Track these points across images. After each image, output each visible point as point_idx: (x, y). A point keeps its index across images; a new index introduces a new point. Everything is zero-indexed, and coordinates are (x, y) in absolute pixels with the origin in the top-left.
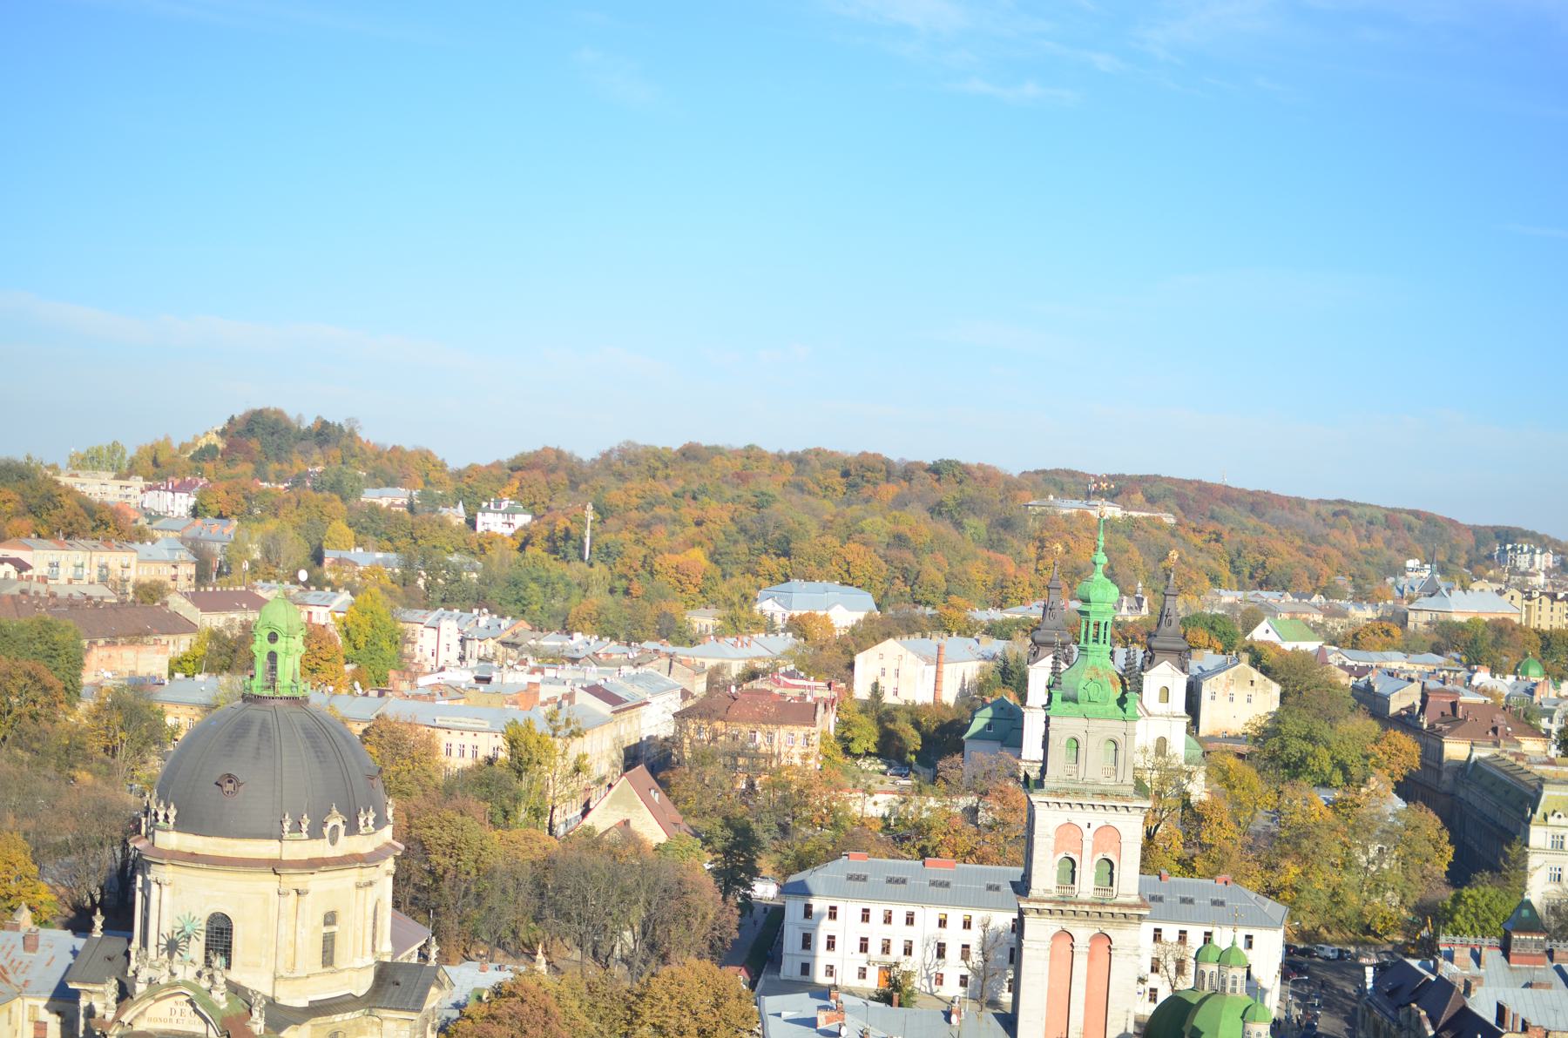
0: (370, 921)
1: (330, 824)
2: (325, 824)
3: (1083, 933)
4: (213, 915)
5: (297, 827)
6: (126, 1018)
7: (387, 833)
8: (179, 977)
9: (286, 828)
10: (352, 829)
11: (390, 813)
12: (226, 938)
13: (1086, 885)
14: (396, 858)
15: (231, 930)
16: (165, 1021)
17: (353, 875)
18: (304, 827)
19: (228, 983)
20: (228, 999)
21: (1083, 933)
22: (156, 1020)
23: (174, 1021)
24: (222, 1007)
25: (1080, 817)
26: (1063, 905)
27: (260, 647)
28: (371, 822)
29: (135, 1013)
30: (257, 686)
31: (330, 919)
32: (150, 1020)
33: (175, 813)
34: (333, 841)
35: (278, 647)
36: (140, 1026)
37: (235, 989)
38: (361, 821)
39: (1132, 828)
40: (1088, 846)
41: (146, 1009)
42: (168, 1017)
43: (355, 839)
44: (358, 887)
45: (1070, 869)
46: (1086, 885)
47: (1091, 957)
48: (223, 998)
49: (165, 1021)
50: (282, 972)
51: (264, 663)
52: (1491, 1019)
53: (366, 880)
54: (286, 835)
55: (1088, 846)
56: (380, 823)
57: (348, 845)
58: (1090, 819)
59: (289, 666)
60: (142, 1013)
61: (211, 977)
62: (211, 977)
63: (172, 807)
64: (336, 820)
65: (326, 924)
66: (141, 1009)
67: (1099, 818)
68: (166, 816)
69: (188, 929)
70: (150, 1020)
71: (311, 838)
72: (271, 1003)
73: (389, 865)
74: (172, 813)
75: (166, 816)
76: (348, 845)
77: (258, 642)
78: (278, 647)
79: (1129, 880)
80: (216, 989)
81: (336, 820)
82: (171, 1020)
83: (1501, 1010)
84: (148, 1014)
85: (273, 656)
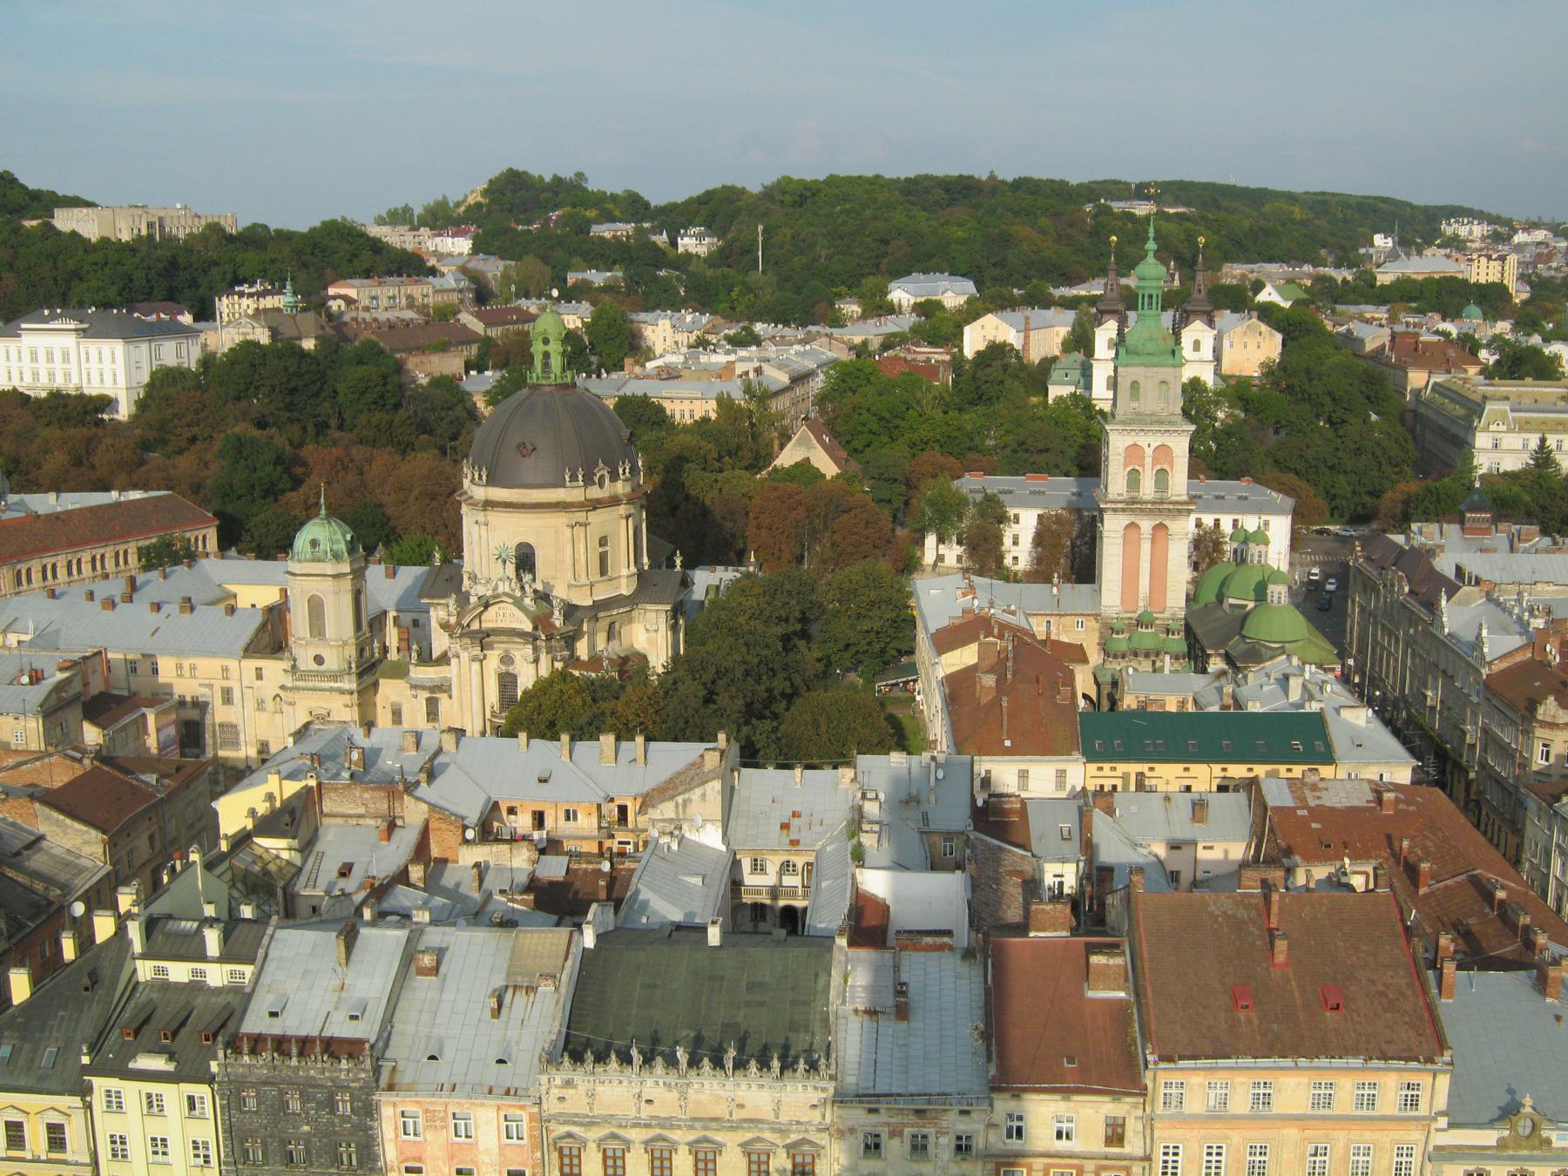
3: (1146, 525)
5: (574, 478)
9: (567, 479)
13: (1147, 490)
18: (580, 477)
21: (1146, 525)
25: (1142, 440)
26: (1133, 505)
31: (603, 541)
34: (601, 486)
38: (621, 471)
39: (1180, 446)
40: (1148, 460)
45: (1134, 479)
46: (1147, 490)
47: (1153, 541)
52: (1450, 573)
54: (568, 484)
55: (1148, 460)
58: (1149, 442)
59: (556, 362)
61: (522, 588)
62: (522, 588)
65: (601, 545)
67: (1156, 440)
68: (480, 477)
75: (480, 477)
79: (1179, 482)
81: (602, 471)
83: (1459, 571)
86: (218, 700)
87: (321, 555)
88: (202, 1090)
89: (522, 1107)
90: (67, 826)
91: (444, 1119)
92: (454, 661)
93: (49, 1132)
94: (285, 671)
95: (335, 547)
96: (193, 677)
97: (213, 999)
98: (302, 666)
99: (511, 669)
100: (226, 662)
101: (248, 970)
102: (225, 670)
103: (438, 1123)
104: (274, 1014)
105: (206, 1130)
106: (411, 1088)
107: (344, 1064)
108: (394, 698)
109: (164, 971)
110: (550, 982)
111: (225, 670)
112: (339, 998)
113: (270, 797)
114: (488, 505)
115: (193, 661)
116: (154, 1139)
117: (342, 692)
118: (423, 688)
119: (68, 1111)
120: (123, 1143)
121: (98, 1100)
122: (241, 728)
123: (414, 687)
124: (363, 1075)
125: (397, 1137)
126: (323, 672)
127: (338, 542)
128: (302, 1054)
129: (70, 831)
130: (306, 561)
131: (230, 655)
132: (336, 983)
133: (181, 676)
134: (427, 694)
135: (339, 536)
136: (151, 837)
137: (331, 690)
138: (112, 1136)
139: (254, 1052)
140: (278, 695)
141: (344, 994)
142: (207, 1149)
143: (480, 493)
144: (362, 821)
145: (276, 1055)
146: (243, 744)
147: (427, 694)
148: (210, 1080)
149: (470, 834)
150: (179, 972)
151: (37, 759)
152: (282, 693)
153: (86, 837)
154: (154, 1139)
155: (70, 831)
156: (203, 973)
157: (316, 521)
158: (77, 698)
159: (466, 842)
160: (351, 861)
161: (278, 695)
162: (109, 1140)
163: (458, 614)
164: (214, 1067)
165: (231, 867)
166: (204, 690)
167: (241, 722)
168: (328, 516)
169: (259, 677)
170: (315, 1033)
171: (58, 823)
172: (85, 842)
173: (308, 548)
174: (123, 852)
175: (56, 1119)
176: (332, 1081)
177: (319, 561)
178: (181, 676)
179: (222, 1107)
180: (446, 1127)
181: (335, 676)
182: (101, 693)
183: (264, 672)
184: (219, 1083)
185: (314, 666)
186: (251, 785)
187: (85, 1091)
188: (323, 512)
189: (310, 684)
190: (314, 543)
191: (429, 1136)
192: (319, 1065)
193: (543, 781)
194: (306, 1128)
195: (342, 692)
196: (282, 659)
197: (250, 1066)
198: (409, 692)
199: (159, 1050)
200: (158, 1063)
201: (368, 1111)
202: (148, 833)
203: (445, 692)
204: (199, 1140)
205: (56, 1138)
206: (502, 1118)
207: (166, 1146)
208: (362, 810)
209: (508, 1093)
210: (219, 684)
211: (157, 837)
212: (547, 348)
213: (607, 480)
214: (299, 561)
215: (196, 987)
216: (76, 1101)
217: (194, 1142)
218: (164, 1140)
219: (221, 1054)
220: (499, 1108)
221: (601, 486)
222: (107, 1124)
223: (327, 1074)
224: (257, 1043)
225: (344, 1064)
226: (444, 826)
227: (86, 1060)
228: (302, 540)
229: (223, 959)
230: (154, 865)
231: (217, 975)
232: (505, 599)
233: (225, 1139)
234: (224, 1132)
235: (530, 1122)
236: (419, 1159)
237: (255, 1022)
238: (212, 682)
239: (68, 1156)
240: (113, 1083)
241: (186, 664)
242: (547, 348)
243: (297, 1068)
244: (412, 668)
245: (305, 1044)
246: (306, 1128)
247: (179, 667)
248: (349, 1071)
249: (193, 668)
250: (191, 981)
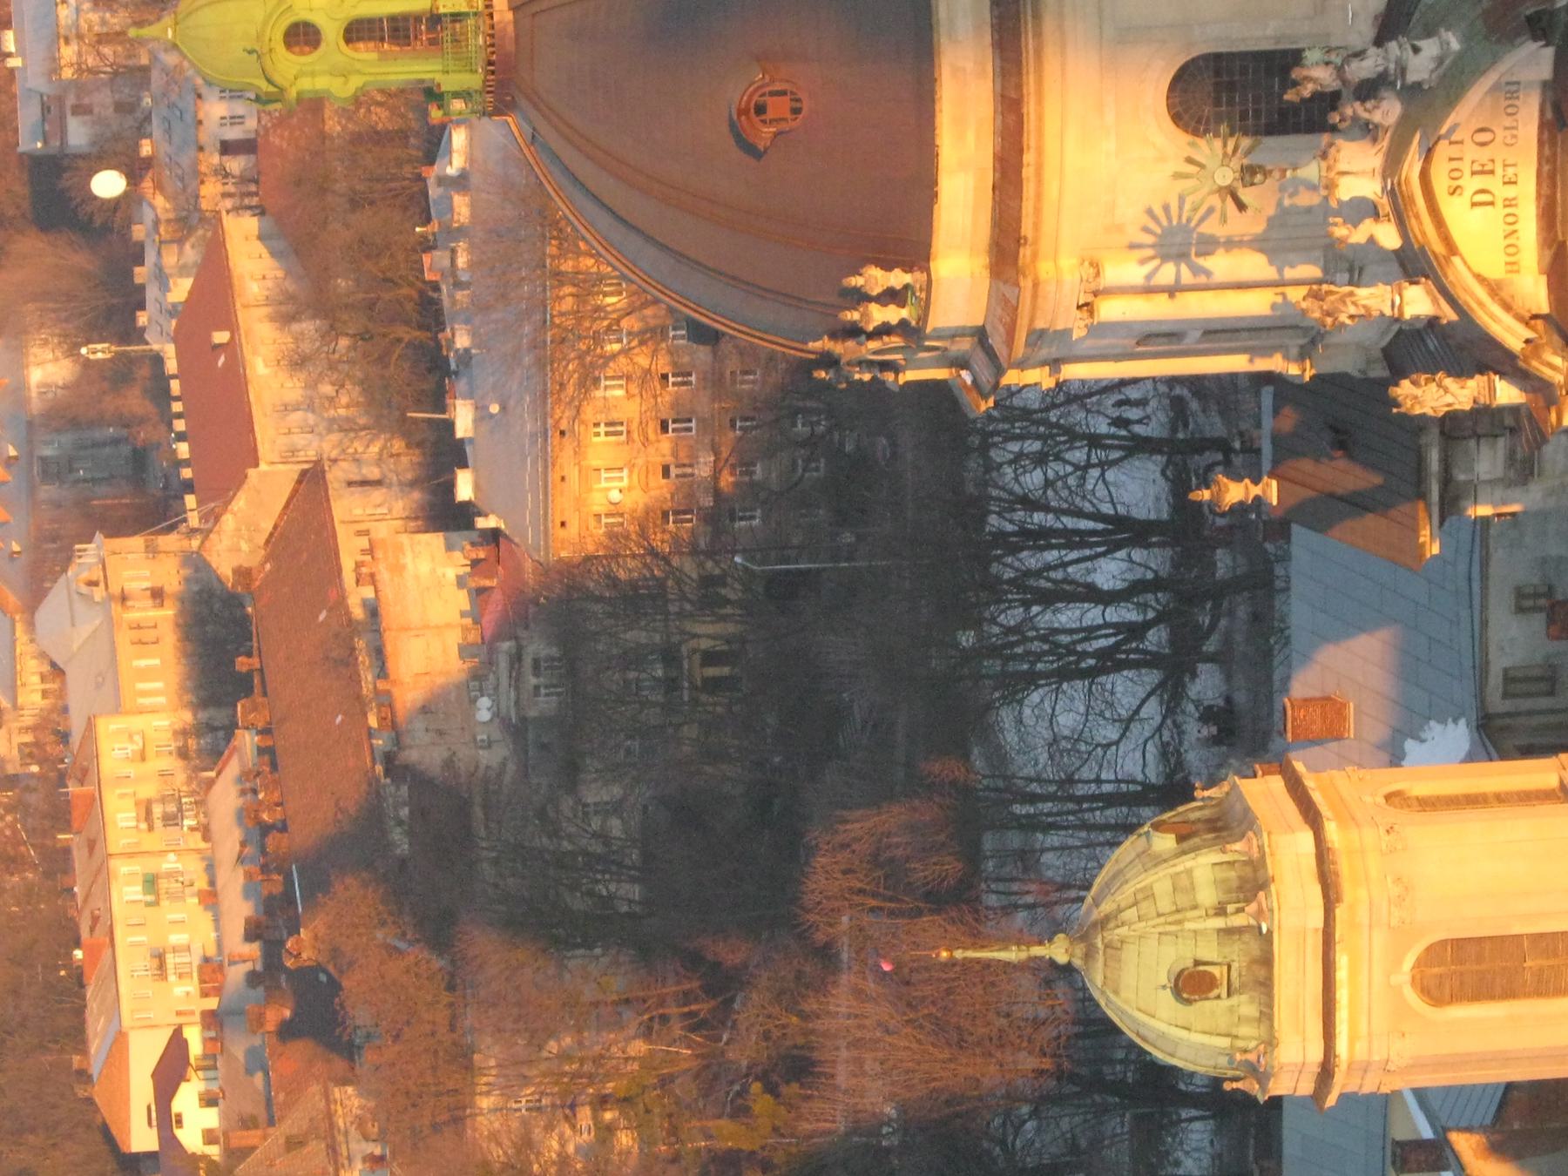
4: (1177, 118)
6: (1512, 335)
8: (1369, 188)
12: (1244, 71)
15: (1218, 57)
16: (1512, 221)
19: (1379, 42)
20: (1429, 33)
22: (1512, 249)
23: (1510, 191)
24: (1455, 45)
29: (1496, 309)
32: (1513, 266)
36: (1535, 291)
41: (1480, 278)
42: (1499, 211)
48: (1430, 48)
49: (1512, 221)
51: (384, 57)
60: (1494, 289)
62: (1368, 90)
63: (856, 281)
66: (1481, 293)
68: (892, 296)
69: (1226, 176)
70: (1513, 266)
74: (876, 278)
75: (892, 296)
77: (321, 83)
80: (1403, 71)
82: (1509, 203)
84: (1495, 271)
85: (358, 31)
87: (1239, 954)
95: (1207, 896)
130: (1266, 1015)
135: (1160, 881)
157: (1096, 979)
163: (1482, 368)
168: (1085, 936)
173: (1211, 1010)
177: (1266, 960)
188: (1058, 951)
212: (332, 31)
214: (1271, 1042)
232: (1412, 167)
242: (332, 31)
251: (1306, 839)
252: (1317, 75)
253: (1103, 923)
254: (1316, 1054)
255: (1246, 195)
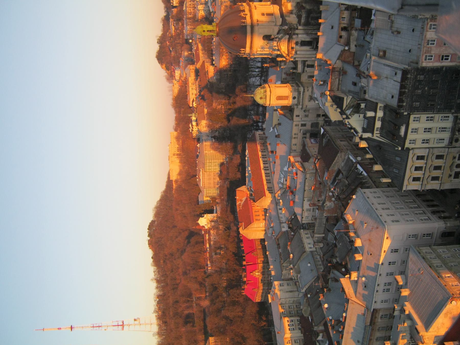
0: (263, 6)
1: (243, 15)
2: (243, 17)
6: (285, 55)
7: (244, 4)
9: (244, 25)
10: (244, 11)
11: (240, 4)
14: (249, 2)
17: (254, 11)
18: (243, 21)
19: (277, 35)
20: (280, 34)
24: (282, 35)
27: (206, 34)
28: (242, 7)
30: (214, 34)
33: (242, 49)
34: (246, 15)
35: (206, 30)
36: (287, 52)
37: (278, 33)
38: (242, 9)
42: (284, 47)
43: (246, 10)
44: (256, 9)
48: (280, 35)
50: (274, 24)
53: (254, 7)
54: (246, 24)
56: (242, 5)
57: (247, 12)
59: (210, 27)
60: (284, 52)
61: (276, 38)
62: (276, 38)
64: (242, 14)
65: (264, 15)
68: (243, 51)
69: (266, 43)
70: (285, 51)
71: (246, 19)
72: (282, 25)
73: (251, 3)
74: (242, 49)
75: (243, 51)
76: (247, 12)
77: (205, 34)
78: (206, 30)
81: (242, 14)
84: (284, 51)
85: (208, 31)
86: (304, 128)
87: (264, 96)
88: (412, 117)
89: (428, 24)
90: (336, 162)
91: (428, 48)
92: (297, 59)
93: (419, 160)
94: (297, 108)
95: (262, 92)
96: (297, 134)
97: (387, 115)
98: (296, 103)
99: (299, 42)
100: (294, 125)
101: (379, 105)
102: (296, 125)
103: (429, 50)
104: (393, 97)
105: (424, 117)
106: (418, 57)
107: (409, 76)
108: (307, 78)
109: (378, 128)
110: (391, 17)
111: (296, 125)
112: (390, 78)
113: (332, 106)
114: (251, 48)
115: (293, 134)
116: (424, 132)
117: (304, 92)
118: (304, 69)
119: (413, 155)
120: (424, 140)
121: (412, 146)
122: (313, 122)
123: (303, 72)
124: (413, 71)
125: (432, 62)
126: (298, 97)
127: (261, 91)
128: (405, 88)
129: (337, 161)
131: (292, 124)
132: (385, 80)
133: (297, 138)
134: (306, 68)
135: (259, 91)
136: (341, 141)
137: (303, 95)
138: (422, 143)
139: (403, 102)
140: (304, 111)
141: (389, 77)
142: (429, 117)
143: (248, 50)
144: (341, 80)
145: (404, 96)
146: (317, 121)
147: (306, 68)
148: (409, 115)
149: (347, 48)
150: (378, 124)
151: (317, 171)
152: (303, 109)
153: (340, 157)
154: (424, 132)
155: (337, 161)
156: (379, 118)
157: (255, 98)
158: (301, 164)
159: (349, 49)
160: (351, 82)
161: (304, 111)
162: (423, 144)
164: (405, 113)
165: (350, 115)
166: (302, 132)
167: (311, 122)
168: (254, 95)
169: (298, 116)
170: (399, 84)
171: (335, 164)
172: (341, 157)
173: (262, 100)
174: (345, 148)
175: (415, 158)
176: (413, 80)
178: (297, 138)
179: (417, 112)
180: (431, 47)
181: (299, 93)
182: (301, 158)
183: (297, 115)
184: (411, 112)
185: (296, 100)
186: (329, 113)
187: (408, 149)
188: (252, 96)
189: (301, 101)
190: (261, 98)
191: (433, 52)
192: (408, 83)
193: (332, 28)
194: (426, 88)
195: (304, 92)
196: (294, 109)
197: (407, 103)
198: (305, 74)
199: (399, 129)
200: (403, 129)
201: (423, 70)
202: (340, 141)
203: (305, 62)
204: (426, 119)
205: (419, 158)
206: (430, 30)
207: (427, 128)
208: (337, 80)
209: (423, 28)
210: (300, 128)
211: (341, 140)
212: (206, 31)
213: (244, 13)
214: (266, 102)
215: (383, 120)
216: (411, 152)
217: (426, 120)
218: (425, 129)
219: (402, 111)
220: (427, 31)
221: (246, 15)
222: (419, 144)
223: (411, 81)
224: (400, 100)
225: (409, 76)
226: (344, 56)
227: (400, 149)
228: (260, 102)
229: (376, 112)
230: (349, 140)
231: (380, 114)
232: (279, 43)
233: (427, 112)
234: (425, 112)
235: (432, 22)
236: (439, 56)
237: (394, 103)
238: (299, 129)
239: (426, 155)
240: (407, 142)
241: (294, 136)
242: (206, 31)
243: (409, 90)
244: (298, 72)
245: (402, 87)
246: (426, 88)
247: (295, 138)
248: (411, 75)
249: (295, 134)
250: (381, 121)
251: (269, 89)
252: (273, 37)
253: (255, 94)
254: (269, 103)
255: (267, 45)
